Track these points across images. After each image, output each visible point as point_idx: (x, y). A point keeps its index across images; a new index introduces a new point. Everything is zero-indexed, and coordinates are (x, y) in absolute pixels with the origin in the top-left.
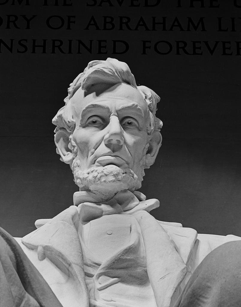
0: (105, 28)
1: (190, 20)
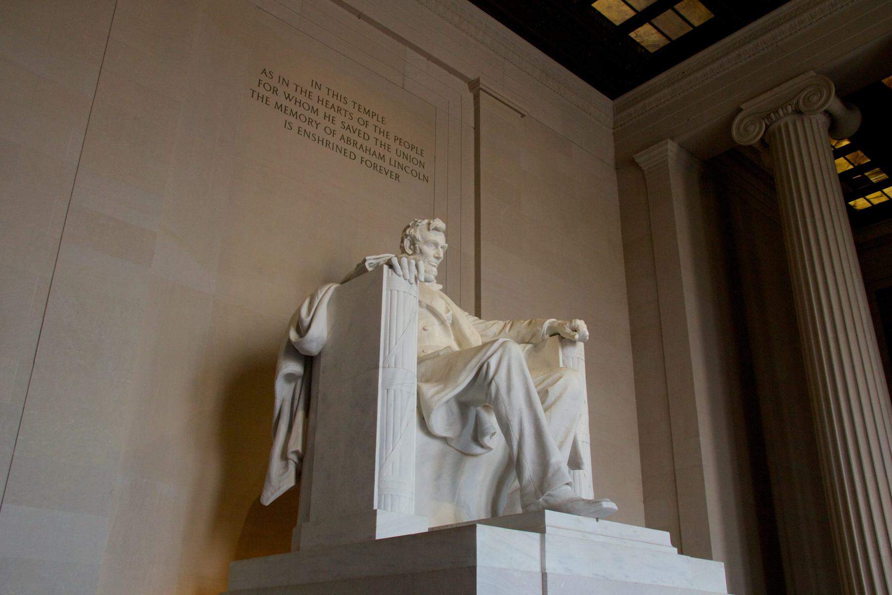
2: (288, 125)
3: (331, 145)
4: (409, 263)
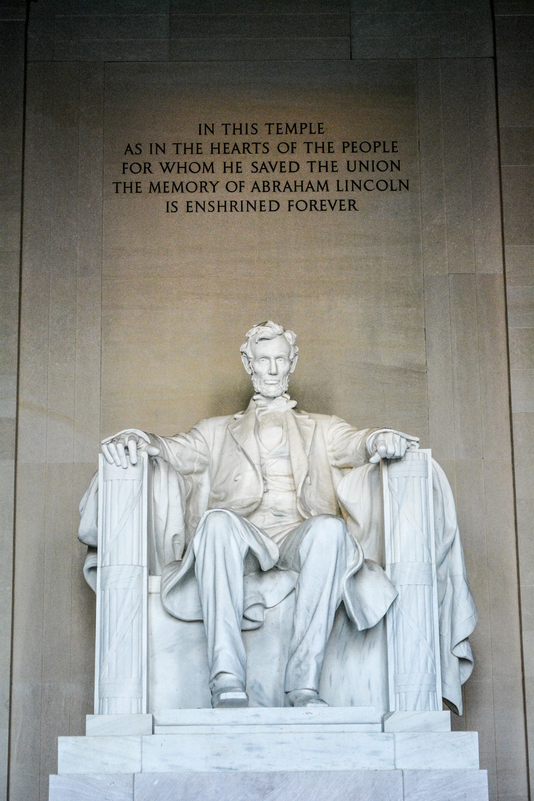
0: (264, 191)
1: (319, 183)
2: (172, 207)
3: (239, 207)
4: (116, 448)
